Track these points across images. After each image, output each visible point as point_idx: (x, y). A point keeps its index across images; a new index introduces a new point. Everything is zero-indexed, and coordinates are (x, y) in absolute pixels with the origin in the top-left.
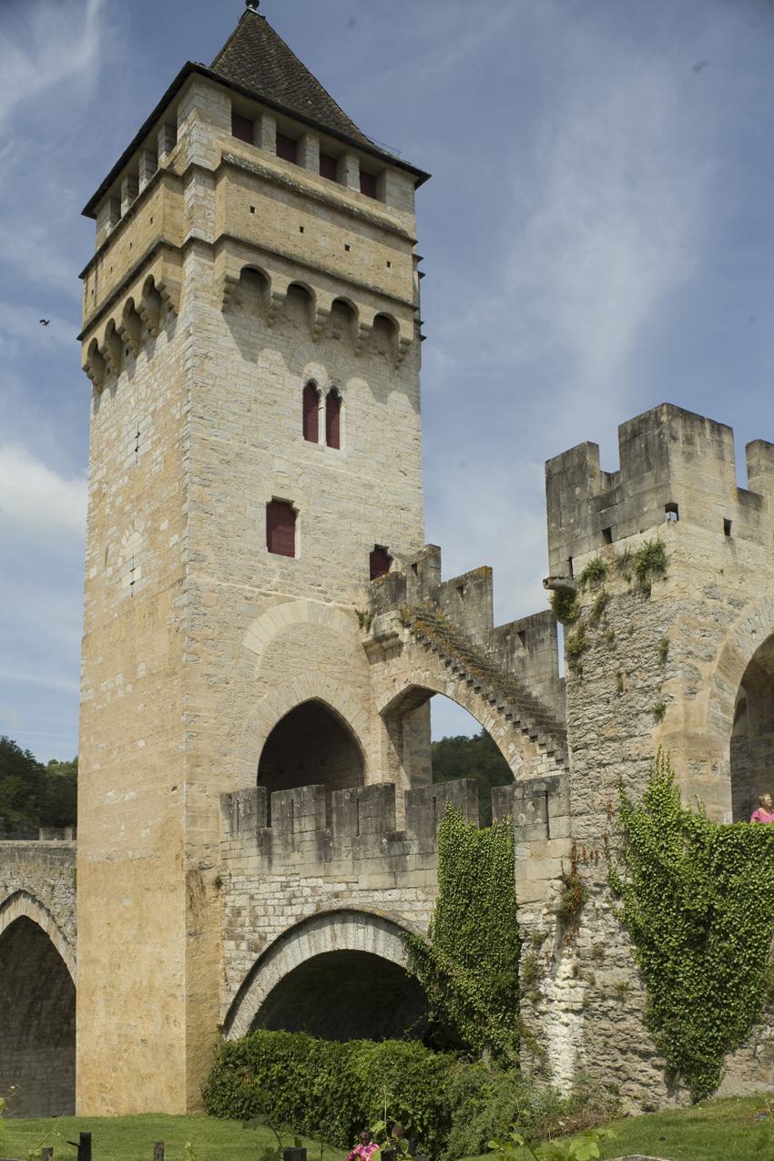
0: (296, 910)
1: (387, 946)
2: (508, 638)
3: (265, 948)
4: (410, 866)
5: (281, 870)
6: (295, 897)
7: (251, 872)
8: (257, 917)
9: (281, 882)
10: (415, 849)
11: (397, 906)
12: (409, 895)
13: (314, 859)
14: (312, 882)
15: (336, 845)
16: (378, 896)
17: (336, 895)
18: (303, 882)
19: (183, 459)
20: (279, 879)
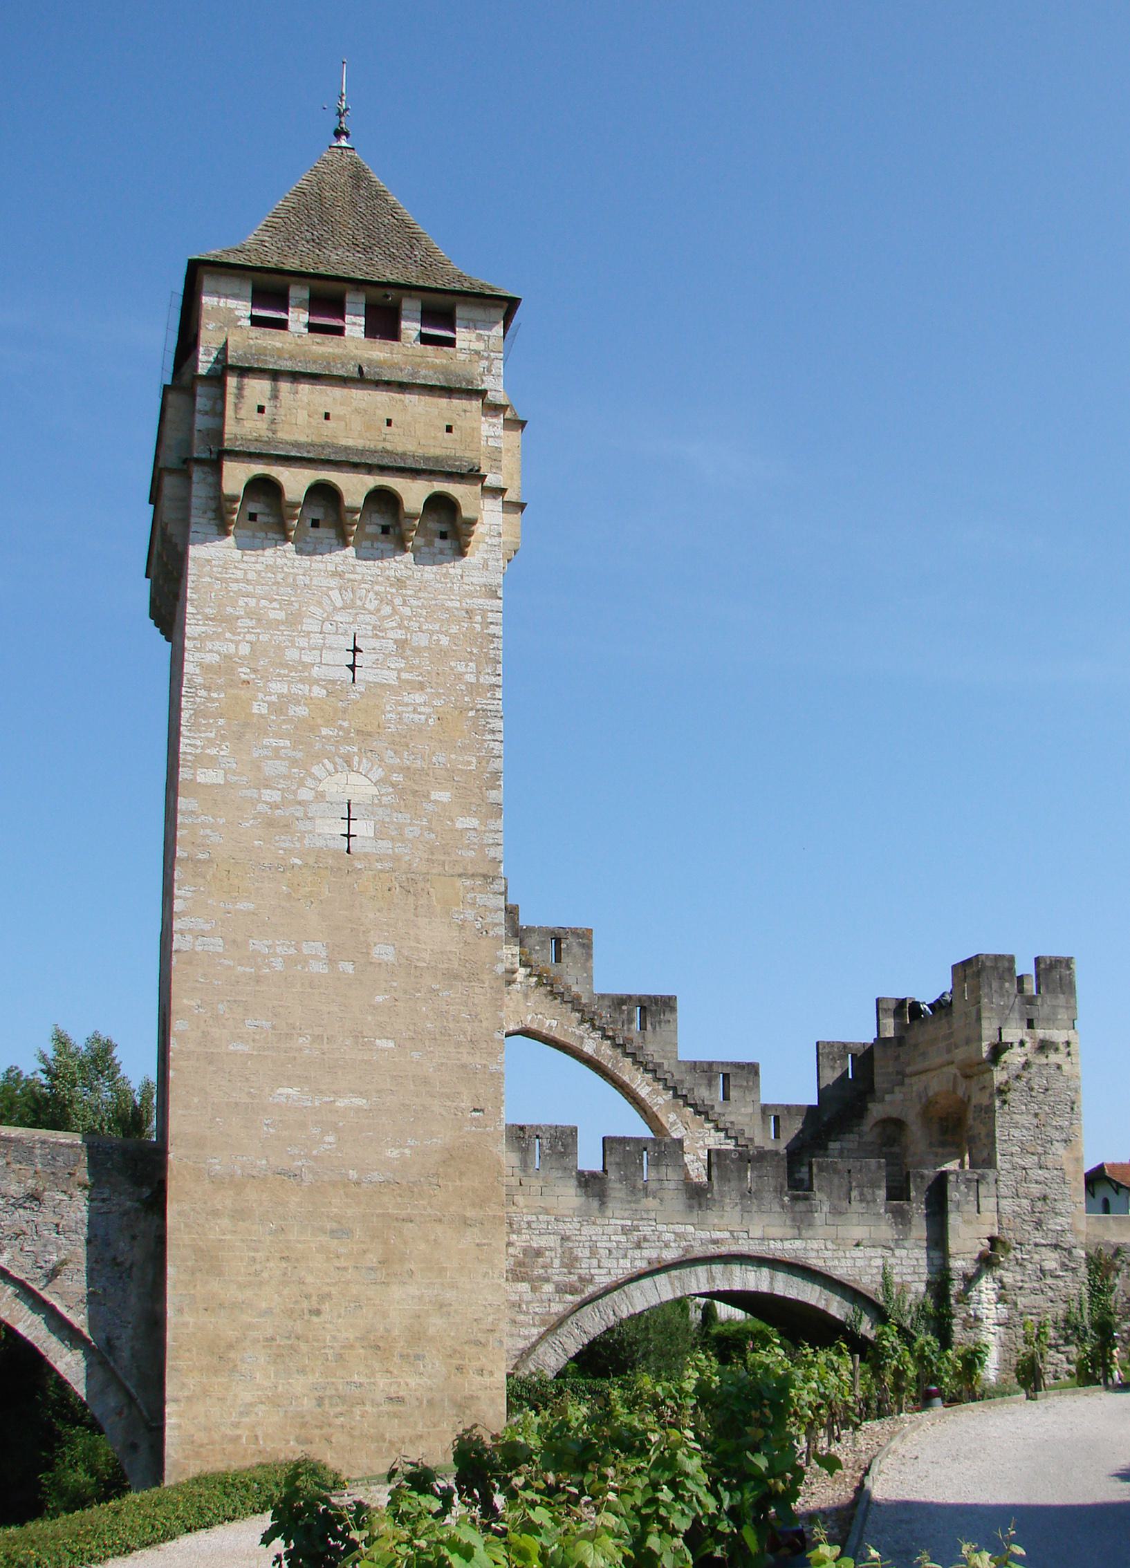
0: (653, 1254)
1: (786, 1285)
2: (624, 1007)
3: (590, 1290)
4: (818, 1222)
5: (626, 1214)
6: (645, 1240)
7: (566, 1212)
8: (576, 1259)
9: (623, 1226)
10: (826, 1208)
11: (801, 1254)
12: (815, 1245)
13: (681, 1207)
14: (680, 1229)
15: (716, 1197)
16: (787, 1244)
17: (715, 1242)
18: (660, 1227)
19: (489, 737)
20: (619, 1222)
